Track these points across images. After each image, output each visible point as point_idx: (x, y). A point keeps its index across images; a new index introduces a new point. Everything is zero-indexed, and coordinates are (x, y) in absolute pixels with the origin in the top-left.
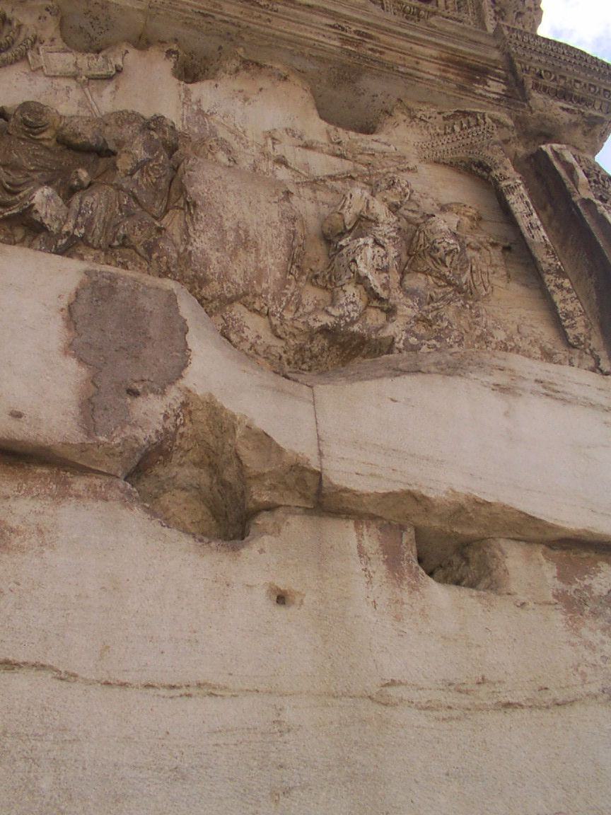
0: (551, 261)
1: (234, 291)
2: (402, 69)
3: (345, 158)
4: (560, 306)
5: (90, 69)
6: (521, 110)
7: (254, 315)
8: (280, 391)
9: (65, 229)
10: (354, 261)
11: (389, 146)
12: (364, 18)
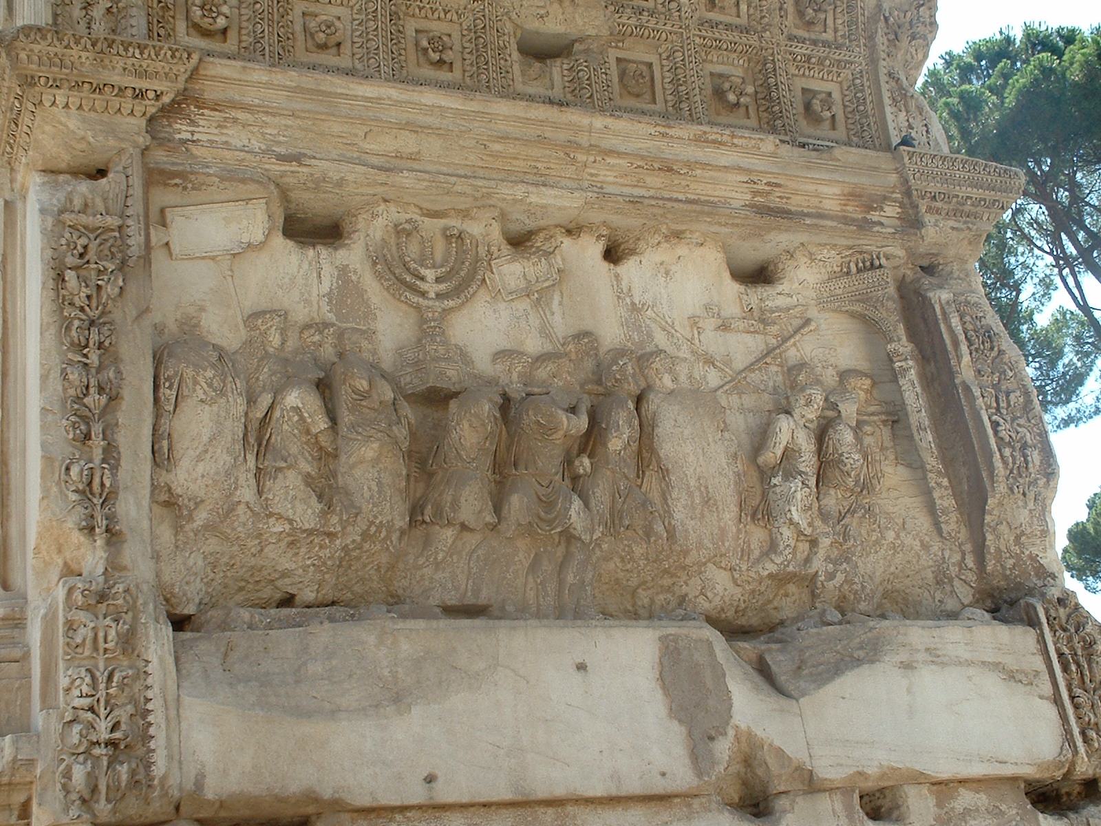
0: (934, 464)
4: (938, 502)
5: (537, 281)
6: (913, 238)
8: (782, 711)
9: (594, 538)
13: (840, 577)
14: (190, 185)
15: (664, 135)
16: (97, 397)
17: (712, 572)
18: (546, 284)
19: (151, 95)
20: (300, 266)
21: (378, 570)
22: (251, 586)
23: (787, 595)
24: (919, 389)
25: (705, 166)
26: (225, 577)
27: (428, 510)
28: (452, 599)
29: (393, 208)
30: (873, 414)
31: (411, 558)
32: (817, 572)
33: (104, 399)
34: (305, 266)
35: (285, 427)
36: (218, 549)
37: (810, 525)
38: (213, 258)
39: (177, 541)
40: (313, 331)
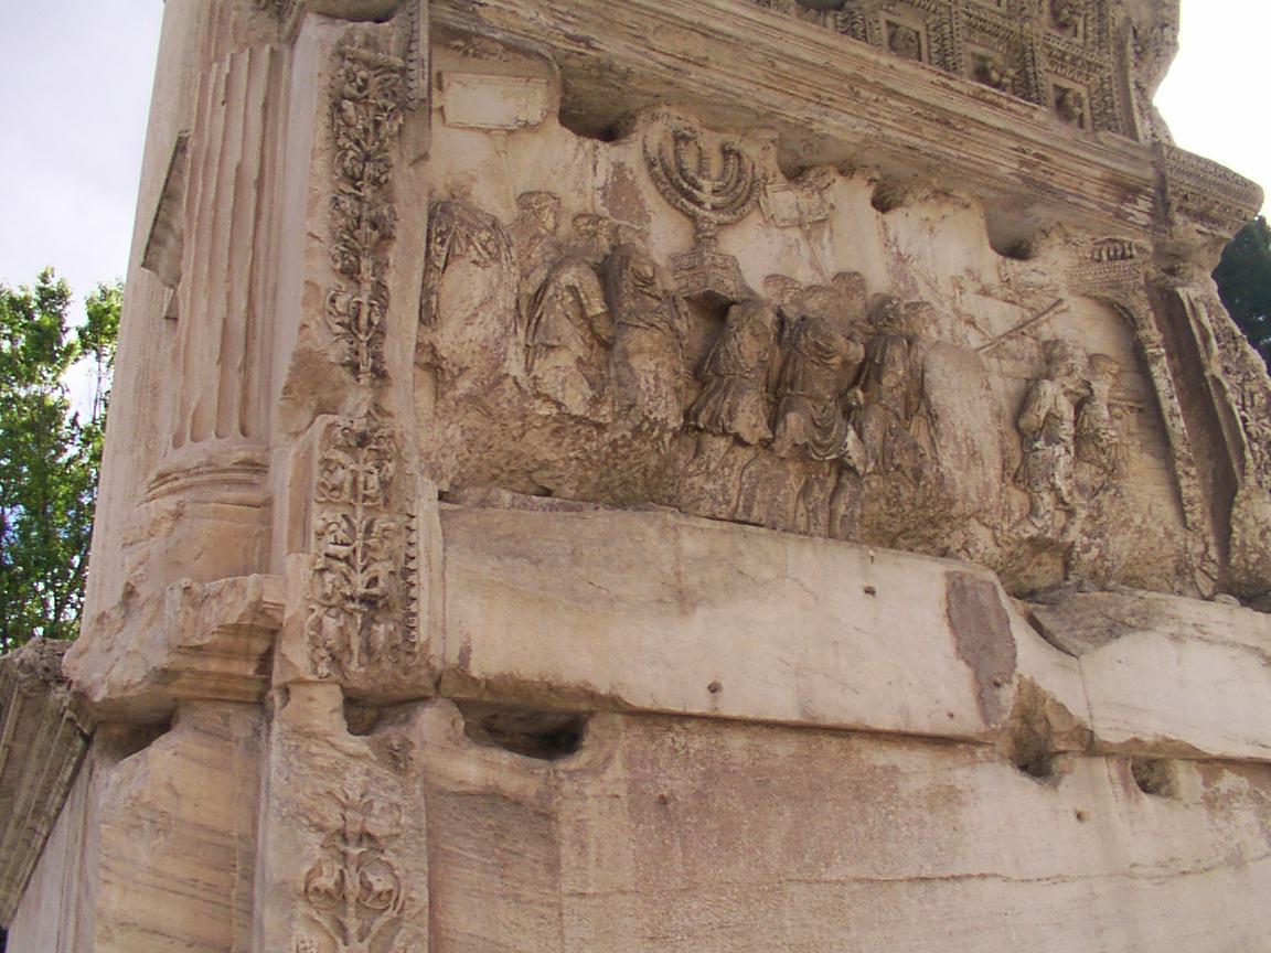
2: (1070, 199)
4: (1185, 491)
5: (810, 213)
8: (1063, 666)
12: (1045, 142)
13: (1095, 551)
14: (471, 51)
15: (945, 86)
16: (369, 230)
17: (974, 525)
18: (818, 218)
20: (575, 157)
21: (644, 474)
22: (504, 476)
23: (1039, 564)
24: (1170, 377)
26: (481, 459)
27: (704, 417)
29: (674, 112)
30: (1119, 399)
31: (681, 464)
32: (1073, 543)
33: (376, 234)
34: (581, 156)
35: (558, 307)
36: (478, 424)
37: (1070, 493)
38: (488, 132)
39: (436, 407)
40: (586, 221)
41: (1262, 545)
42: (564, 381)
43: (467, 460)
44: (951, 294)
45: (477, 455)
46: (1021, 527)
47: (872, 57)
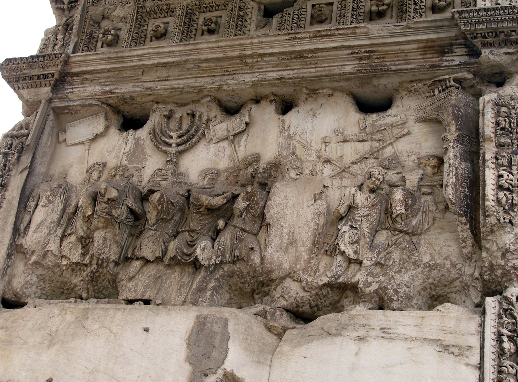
1: (284, 273)
2: (394, 68)
3: (366, 141)
5: (233, 130)
7: (295, 282)
8: (259, 362)
10: (338, 244)
11: (397, 116)
14: (73, 112)
15: (295, 39)
19: (50, 76)
21: (109, 282)
25: (322, 50)
28: (131, 297)
29: (160, 106)
34: (121, 140)
36: (43, 273)
38: (82, 143)
41: (503, 263)
42: (71, 248)
43: (45, 288)
44: (318, 147)
45: (48, 285)
46: (320, 278)
47: (249, 41)
